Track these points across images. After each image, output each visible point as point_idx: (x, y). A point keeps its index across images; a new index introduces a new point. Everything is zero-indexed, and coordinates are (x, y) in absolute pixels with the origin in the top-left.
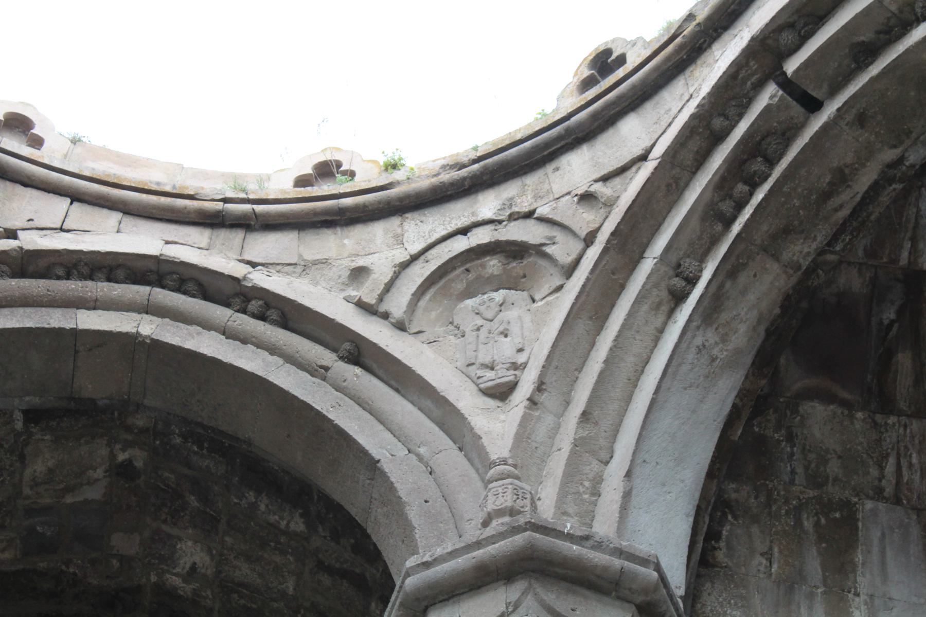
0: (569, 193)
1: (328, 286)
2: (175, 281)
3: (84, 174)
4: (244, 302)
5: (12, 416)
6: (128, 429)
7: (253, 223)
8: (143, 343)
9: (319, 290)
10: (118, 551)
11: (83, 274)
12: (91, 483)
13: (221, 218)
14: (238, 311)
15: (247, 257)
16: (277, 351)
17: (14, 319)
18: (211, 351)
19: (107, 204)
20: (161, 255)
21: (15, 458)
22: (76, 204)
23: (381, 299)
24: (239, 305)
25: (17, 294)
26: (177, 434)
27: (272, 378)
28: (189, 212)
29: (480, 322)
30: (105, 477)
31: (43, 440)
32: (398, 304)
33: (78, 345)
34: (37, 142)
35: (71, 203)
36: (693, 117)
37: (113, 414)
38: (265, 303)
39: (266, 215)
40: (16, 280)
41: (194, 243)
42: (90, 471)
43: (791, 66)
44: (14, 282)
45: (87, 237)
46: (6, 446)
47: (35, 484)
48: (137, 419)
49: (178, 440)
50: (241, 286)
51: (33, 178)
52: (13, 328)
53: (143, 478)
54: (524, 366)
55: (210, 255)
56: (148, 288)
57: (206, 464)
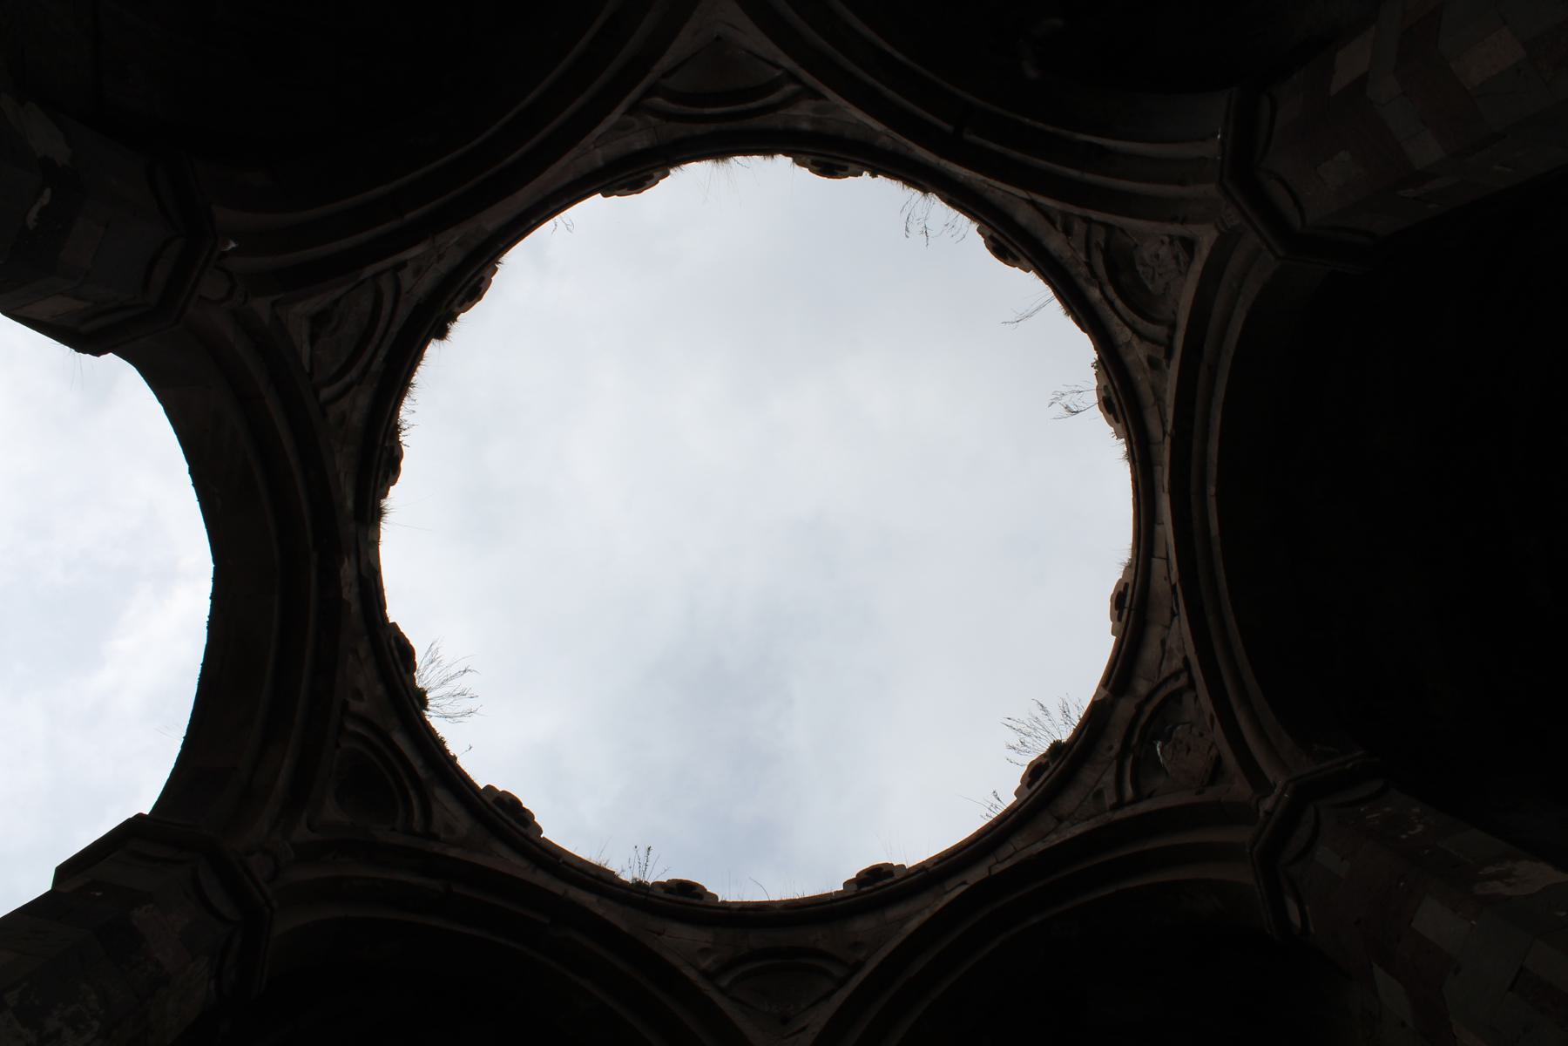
0: (1069, 244)
23: (1161, 345)
29: (1157, 276)
32: (1159, 331)
36: (996, 180)
43: (948, 128)
45: (1169, 540)
54: (1170, 236)
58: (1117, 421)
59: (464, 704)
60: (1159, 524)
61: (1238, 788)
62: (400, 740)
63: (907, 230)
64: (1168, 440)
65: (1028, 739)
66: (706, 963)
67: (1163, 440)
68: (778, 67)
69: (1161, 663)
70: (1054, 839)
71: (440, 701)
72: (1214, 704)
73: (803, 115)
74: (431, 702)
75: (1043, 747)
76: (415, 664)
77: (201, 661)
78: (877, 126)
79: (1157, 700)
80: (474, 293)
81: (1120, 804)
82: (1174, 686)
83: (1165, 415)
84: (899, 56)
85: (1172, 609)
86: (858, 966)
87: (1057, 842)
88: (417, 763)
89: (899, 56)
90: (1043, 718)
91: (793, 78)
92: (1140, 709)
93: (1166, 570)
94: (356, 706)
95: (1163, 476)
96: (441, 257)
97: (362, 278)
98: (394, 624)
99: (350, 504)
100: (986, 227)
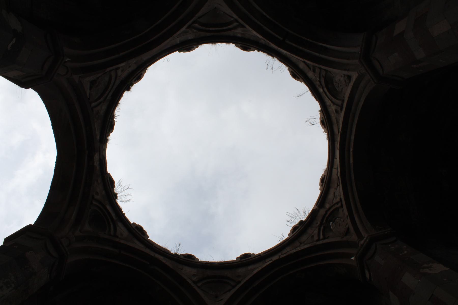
0: (314, 75)
15: (338, 133)
29: (339, 86)
32: (339, 102)
36: (294, 55)
43: (281, 39)
45: (338, 164)
54: (344, 75)
58: (325, 128)
59: (128, 198)
60: (335, 159)
61: (353, 237)
62: (109, 207)
63: (267, 68)
64: (339, 134)
65: (293, 219)
66: (194, 279)
67: (338, 134)
68: (232, 17)
69: (333, 199)
70: (299, 249)
71: (121, 197)
73: (239, 32)
74: (118, 197)
75: (297, 222)
76: (114, 185)
77: (52, 181)
78: (260, 37)
79: (331, 210)
80: (139, 78)
81: (318, 240)
83: (339, 127)
84: (268, 17)
86: (239, 282)
87: (300, 250)
88: (113, 215)
89: (268, 17)
90: (298, 213)
91: (237, 21)
92: (326, 212)
93: (336, 172)
94: (96, 197)
95: (338, 145)
96: (130, 67)
97: (106, 71)
98: (109, 174)
99: (98, 137)
100: (290, 68)
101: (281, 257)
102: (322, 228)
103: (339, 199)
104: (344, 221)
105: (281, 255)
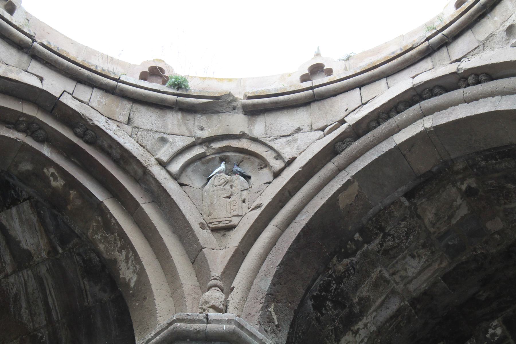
1: (500, 46)
2: (428, 93)
3: (358, 72)
4: (465, 81)
5: (401, 201)
6: (457, 173)
7: (447, 41)
8: (431, 132)
9: (497, 51)
10: (494, 230)
11: (385, 118)
12: (459, 207)
13: (431, 49)
14: (465, 87)
16: (494, 94)
17: (367, 159)
18: (464, 115)
19: (376, 78)
20: (413, 85)
21: (416, 219)
22: (362, 88)
24: (464, 84)
25: (361, 147)
26: (481, 161)
27: (500, 108)
28: (415, 57)
30: (463, 201)
31: (422, 203)
33: (402, 152)
34: (329, 72)
35: (360, 89)
37: (445, 170)
38: (475, 75)
39: (451, 33)
40: (357, 141)
41: (426, 69)
42: (454, 203)
44: (356, 143)
45: (376, 100)
46: (408, 216)
47: (433, 225)
48: (458, 166)
49: (483, 163)
50: (459, 74)
51: (337, 90)
52: (369, 164)
53: (480, 190)
55: (436, 69)
56: (418, 105)
57: (504, 165)
72: (270, 204)
81: (163, 164)
82: (269, 156)
85: (326, 126)
101: (67, 100)
102: (198, 151)
103: (291, 157)
104: (244, 201)
105: (69, 93)
